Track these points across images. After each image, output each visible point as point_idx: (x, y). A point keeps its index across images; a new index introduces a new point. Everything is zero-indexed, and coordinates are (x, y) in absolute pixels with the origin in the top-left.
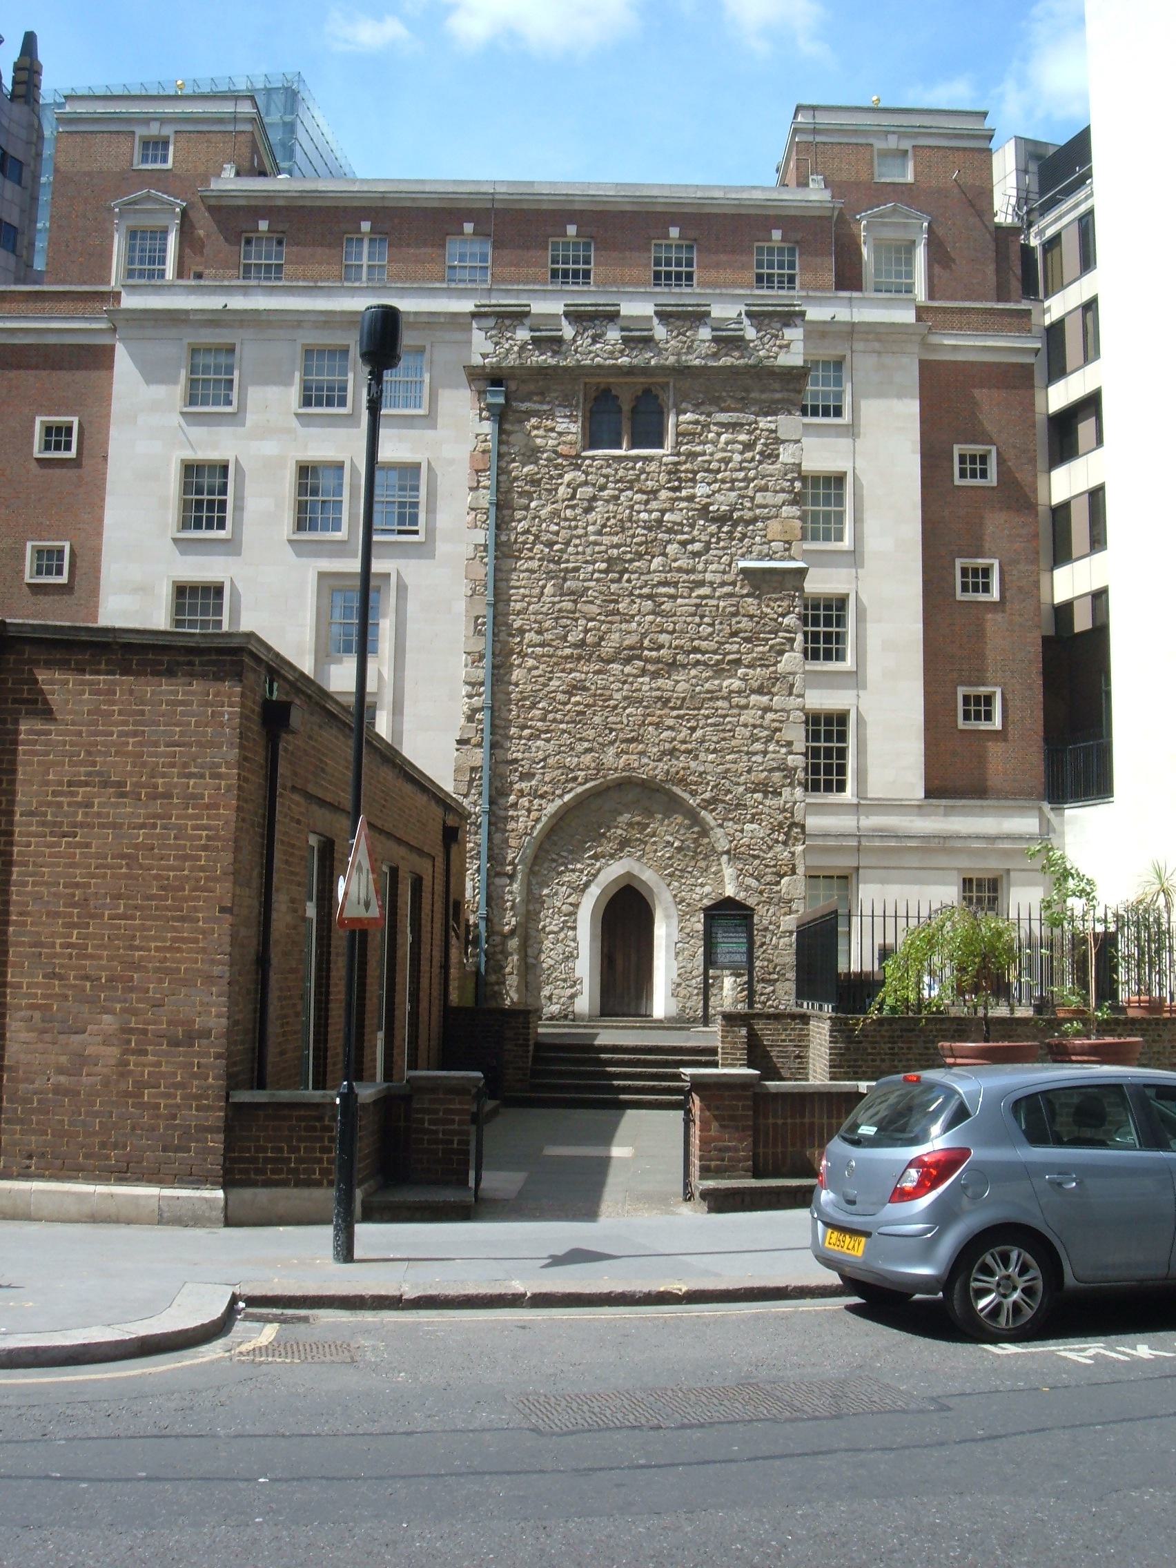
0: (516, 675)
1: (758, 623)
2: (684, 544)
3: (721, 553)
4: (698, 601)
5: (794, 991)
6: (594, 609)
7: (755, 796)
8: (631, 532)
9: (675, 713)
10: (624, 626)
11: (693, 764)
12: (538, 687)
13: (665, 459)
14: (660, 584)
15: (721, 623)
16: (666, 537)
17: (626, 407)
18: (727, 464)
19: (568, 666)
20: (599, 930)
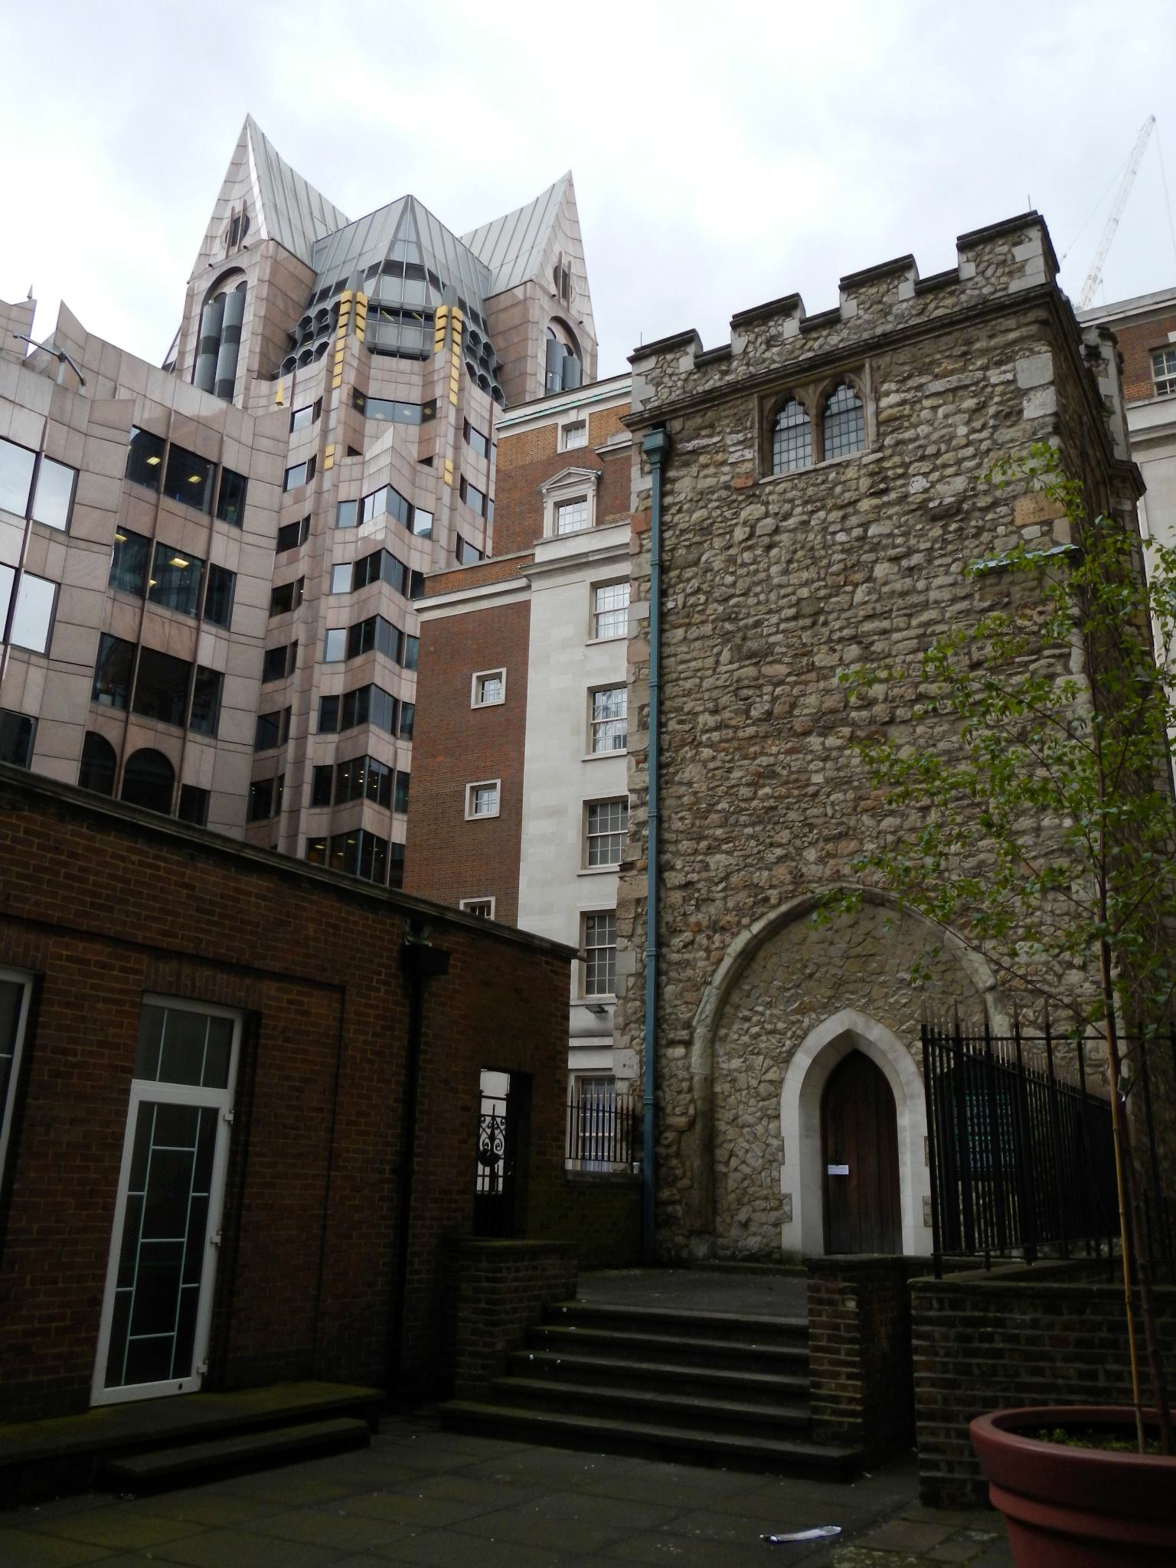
0: (691, 772)
2: (895, 560)
3: (948, 560)
4: (920, 631)
6: (781, 670)
8: (825, 562)
10: (822, 685)
13: (865, 460)
14: (868, 618)
15: (956, 654)
16: (872, 557)
18: (951, 439)
19: (752, 750)
20: (816, 1122)
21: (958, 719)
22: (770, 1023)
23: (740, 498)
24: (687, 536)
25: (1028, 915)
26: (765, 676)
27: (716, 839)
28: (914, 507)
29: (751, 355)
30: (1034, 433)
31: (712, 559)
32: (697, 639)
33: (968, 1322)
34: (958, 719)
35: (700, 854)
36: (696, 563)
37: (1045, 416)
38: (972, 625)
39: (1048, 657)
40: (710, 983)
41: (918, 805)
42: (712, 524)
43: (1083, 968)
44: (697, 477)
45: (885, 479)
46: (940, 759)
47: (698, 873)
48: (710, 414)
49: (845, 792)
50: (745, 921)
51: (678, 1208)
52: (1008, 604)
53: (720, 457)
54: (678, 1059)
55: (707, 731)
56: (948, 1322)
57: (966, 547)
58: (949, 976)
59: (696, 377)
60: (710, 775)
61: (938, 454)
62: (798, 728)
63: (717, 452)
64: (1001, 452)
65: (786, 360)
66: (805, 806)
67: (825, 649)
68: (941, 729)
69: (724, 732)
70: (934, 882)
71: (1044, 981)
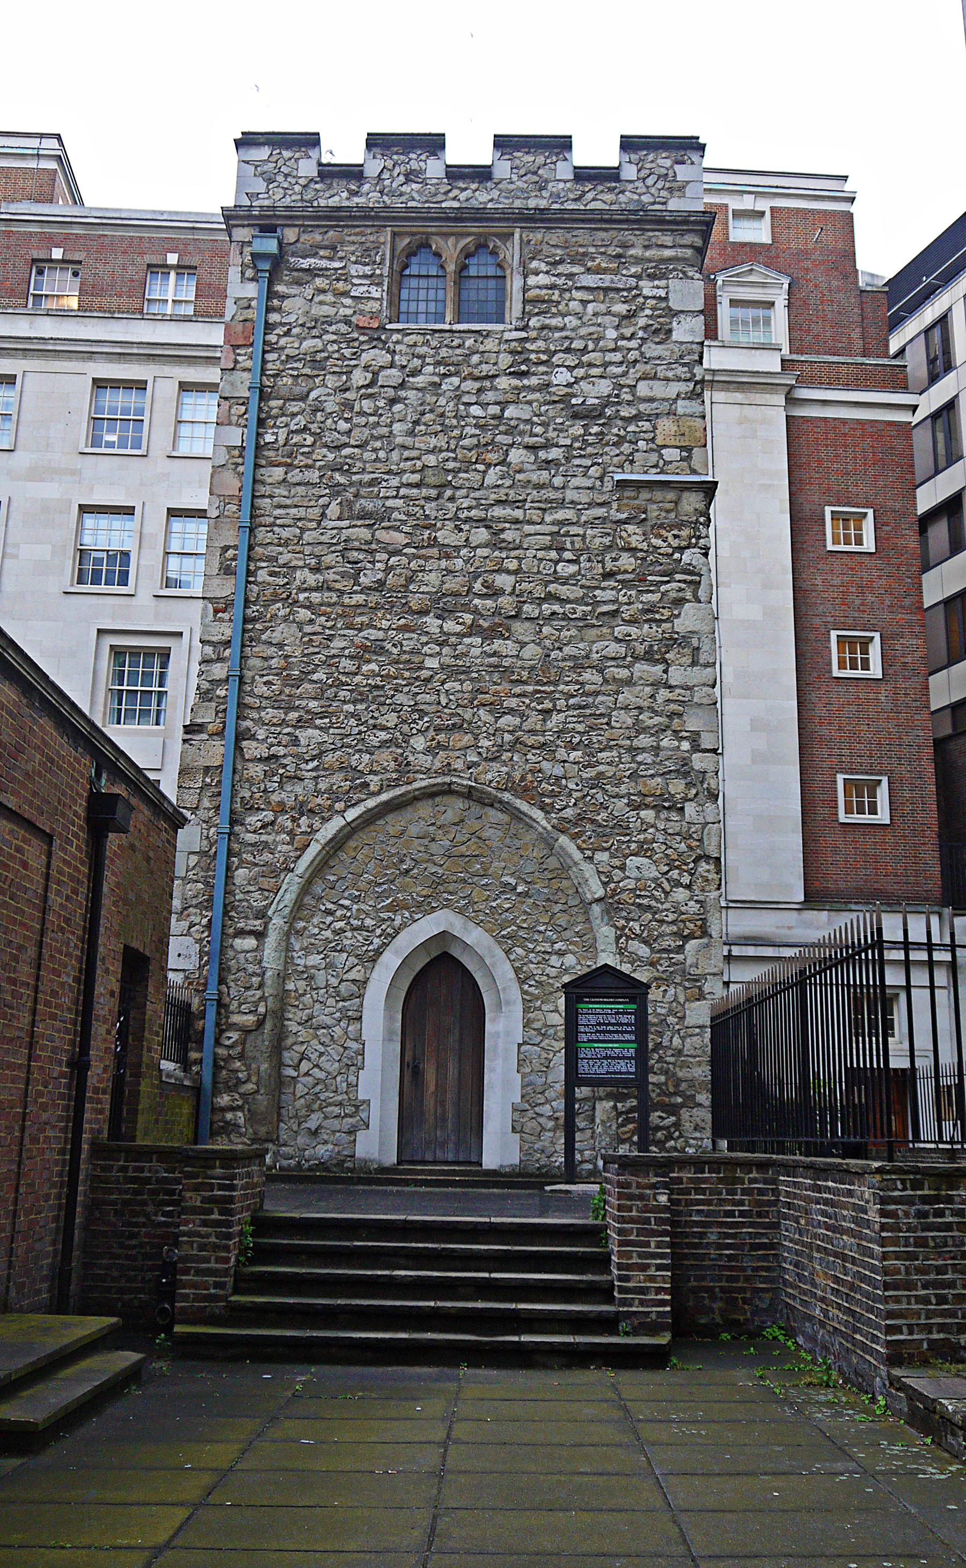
1: (644, 559)
4: (555, 529)
5: (709, 1126)
6: (399, 538)
7: (643, 813)
8: (456, 432)
9: (518, 690)
10: (444, 563)
11: (545, 765)
12: (311, 650)
13: (507, 336)
14: (499, 502)
15: (589, 560)
16: (508, 440)
17: (451, 268)
18: (598, 339)
19: (359, 619)
21: (587, 626)
22: (357, 918)
23: (362, 338)
24: (295, 365)
25: (641, 832)
26: (379, 542)
27: (308, 712)
28: (556, 399)
29: (387, 183)
30: (681, 357)
31: (323, 398)
32: (299, 484)
33: (925, 1200)
34: (587, 626)
35: (288, 726)
36: (304, 398)
37: (692, 343)
38: (608, 534)
39: (679, 581)
40: (292, 871)
41: (539, 707)
42: (327, 358)
43: (688, 887)
44: (311, 300)
45: (526, 361)
46: (565, 664)
47: (285, 746)
48: (331, 233)
49: (462, 682)
50: (339, 806)
51: (240, 1114)
52: (644, 520)
53: (340, 285)
54: (248, 952)
55: (306, 590)
56: (909, 1201)
57: (607, 454)
58: (555, 884)
59: (317, 186)
60: (306, 639)
61: (584, 351)
62: (415, 607)
63: (338, 280)
64: (648, 367)
65: (426, 202)
66: (416, 690)
67: (450, 525)
68: (568, 633)
69: (326, 594)
70: (550, 788)
71: (652, 897)
